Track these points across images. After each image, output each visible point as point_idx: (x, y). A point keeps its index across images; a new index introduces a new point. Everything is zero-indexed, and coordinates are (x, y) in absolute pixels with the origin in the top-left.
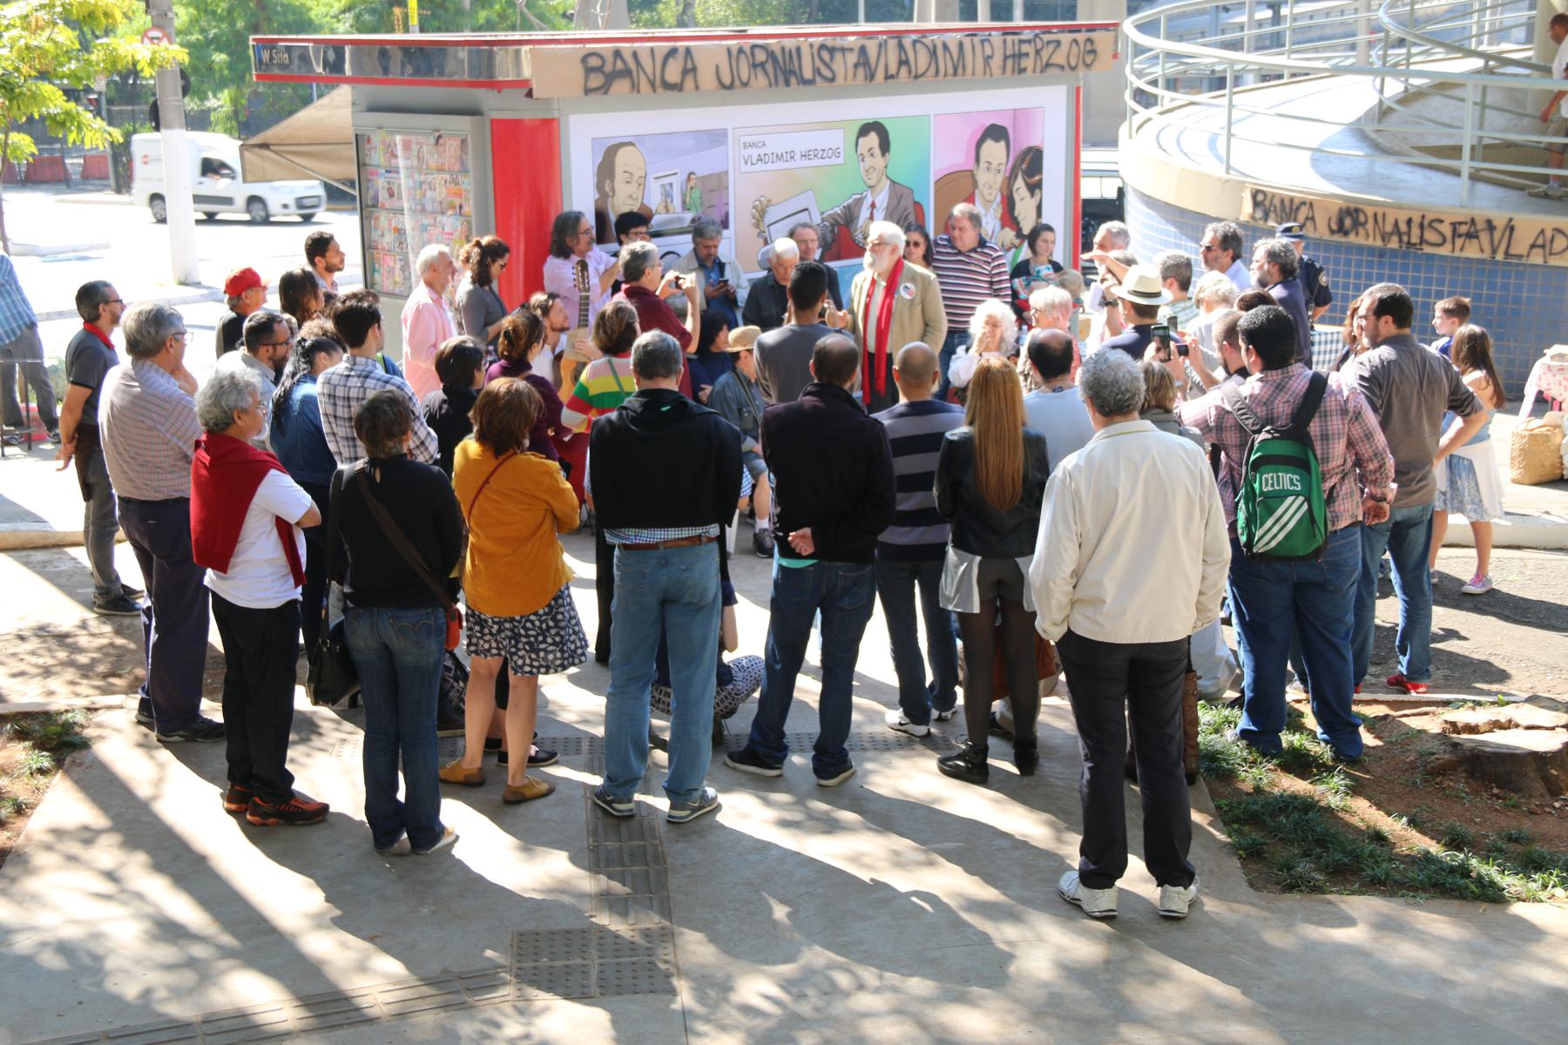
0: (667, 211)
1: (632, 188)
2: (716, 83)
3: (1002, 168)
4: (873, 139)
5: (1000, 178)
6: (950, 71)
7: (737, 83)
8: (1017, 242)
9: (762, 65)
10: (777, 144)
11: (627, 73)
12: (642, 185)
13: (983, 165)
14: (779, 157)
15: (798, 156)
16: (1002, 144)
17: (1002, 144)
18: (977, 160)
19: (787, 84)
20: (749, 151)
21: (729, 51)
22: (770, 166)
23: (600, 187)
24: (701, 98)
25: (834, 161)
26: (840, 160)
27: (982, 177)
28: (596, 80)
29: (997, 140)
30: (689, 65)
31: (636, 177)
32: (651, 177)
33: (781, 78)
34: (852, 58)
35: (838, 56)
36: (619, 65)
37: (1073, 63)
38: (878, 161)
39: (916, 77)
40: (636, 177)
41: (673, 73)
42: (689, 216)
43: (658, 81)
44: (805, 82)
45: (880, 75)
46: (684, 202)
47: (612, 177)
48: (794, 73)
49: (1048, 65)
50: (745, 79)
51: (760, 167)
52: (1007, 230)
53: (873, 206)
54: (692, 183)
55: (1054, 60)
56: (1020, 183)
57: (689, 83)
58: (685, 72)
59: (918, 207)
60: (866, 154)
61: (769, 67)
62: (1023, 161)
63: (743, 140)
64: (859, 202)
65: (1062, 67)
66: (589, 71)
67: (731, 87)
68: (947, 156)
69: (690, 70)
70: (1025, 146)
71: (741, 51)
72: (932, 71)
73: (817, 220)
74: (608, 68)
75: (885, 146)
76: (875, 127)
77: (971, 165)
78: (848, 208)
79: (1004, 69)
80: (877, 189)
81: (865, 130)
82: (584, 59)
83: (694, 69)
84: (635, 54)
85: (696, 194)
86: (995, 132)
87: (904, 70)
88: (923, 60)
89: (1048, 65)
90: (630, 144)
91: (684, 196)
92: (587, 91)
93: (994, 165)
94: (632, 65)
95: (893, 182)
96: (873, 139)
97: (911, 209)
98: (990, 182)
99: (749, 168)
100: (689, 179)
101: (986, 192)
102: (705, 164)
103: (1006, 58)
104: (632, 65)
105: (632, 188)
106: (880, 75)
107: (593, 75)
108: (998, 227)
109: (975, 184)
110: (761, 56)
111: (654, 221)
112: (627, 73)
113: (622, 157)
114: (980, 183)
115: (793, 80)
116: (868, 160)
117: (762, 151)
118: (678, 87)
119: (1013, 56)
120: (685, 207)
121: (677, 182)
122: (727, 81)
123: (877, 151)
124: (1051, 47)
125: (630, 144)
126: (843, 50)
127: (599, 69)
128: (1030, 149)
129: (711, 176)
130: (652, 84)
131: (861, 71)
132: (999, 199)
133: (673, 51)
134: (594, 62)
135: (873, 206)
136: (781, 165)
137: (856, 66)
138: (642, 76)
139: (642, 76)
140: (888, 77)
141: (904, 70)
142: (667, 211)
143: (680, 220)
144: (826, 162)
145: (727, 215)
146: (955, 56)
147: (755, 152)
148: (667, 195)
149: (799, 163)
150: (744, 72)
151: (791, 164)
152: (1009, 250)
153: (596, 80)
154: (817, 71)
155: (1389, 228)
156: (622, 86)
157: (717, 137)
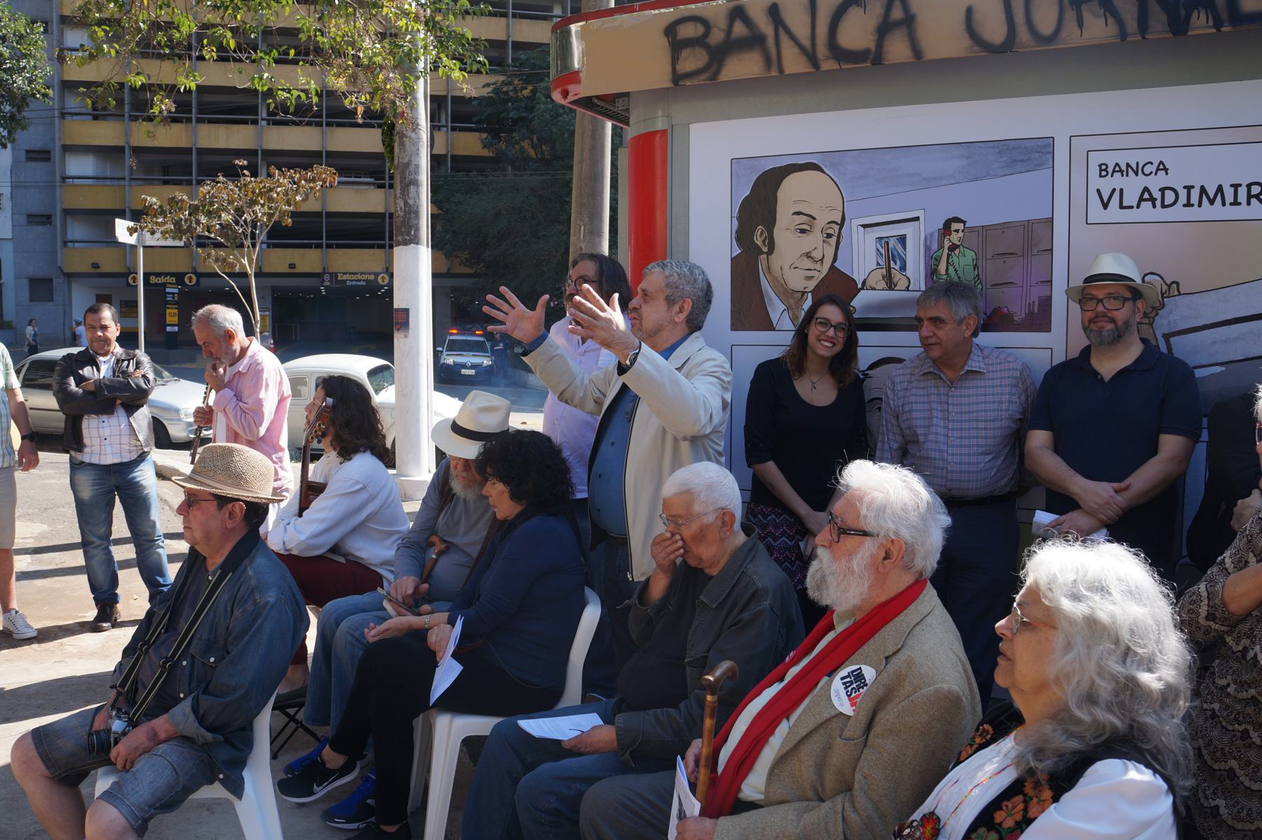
0: (891, 285)
1: (813, 241)
2: (966, 41)
7: (1023, 34)
10: (1191, 168)
11: (755, 41)
12: (836, 231)
20: (1107, 185)
22: (1178, 212)
23: (743, 236)
28: (692, 60)
30: (897, 13)
31: (821, 222)
32: (855, 223)
36: (739, 29)
40: (821, 222)
43: (822, 50)
47: (770, 222)
50: (1046, 27)
54: (955, 238)
57: (897, 49)
58: (884, 29)
63: (1096, 159)
66: (677, 47)
74: (717, 37)
83: (909, 21)
85: (964, 259)
92: (677, 78)
94: (766, 28)
102: (993, 203)
104: (766, 28)
105: (813, 241)
107: (685, 53)
112: (755, 41)
113: (791, 192)
117: (1155, 183)
122: (995, 31)
129: (1004, 227)
138: (786, 43)
139: (786, 43)
142: (891, 285)
145: (1046, 303)
147: (1132, 186)
148: (891, 256)
153: (692, 60)
156: (743, 66)
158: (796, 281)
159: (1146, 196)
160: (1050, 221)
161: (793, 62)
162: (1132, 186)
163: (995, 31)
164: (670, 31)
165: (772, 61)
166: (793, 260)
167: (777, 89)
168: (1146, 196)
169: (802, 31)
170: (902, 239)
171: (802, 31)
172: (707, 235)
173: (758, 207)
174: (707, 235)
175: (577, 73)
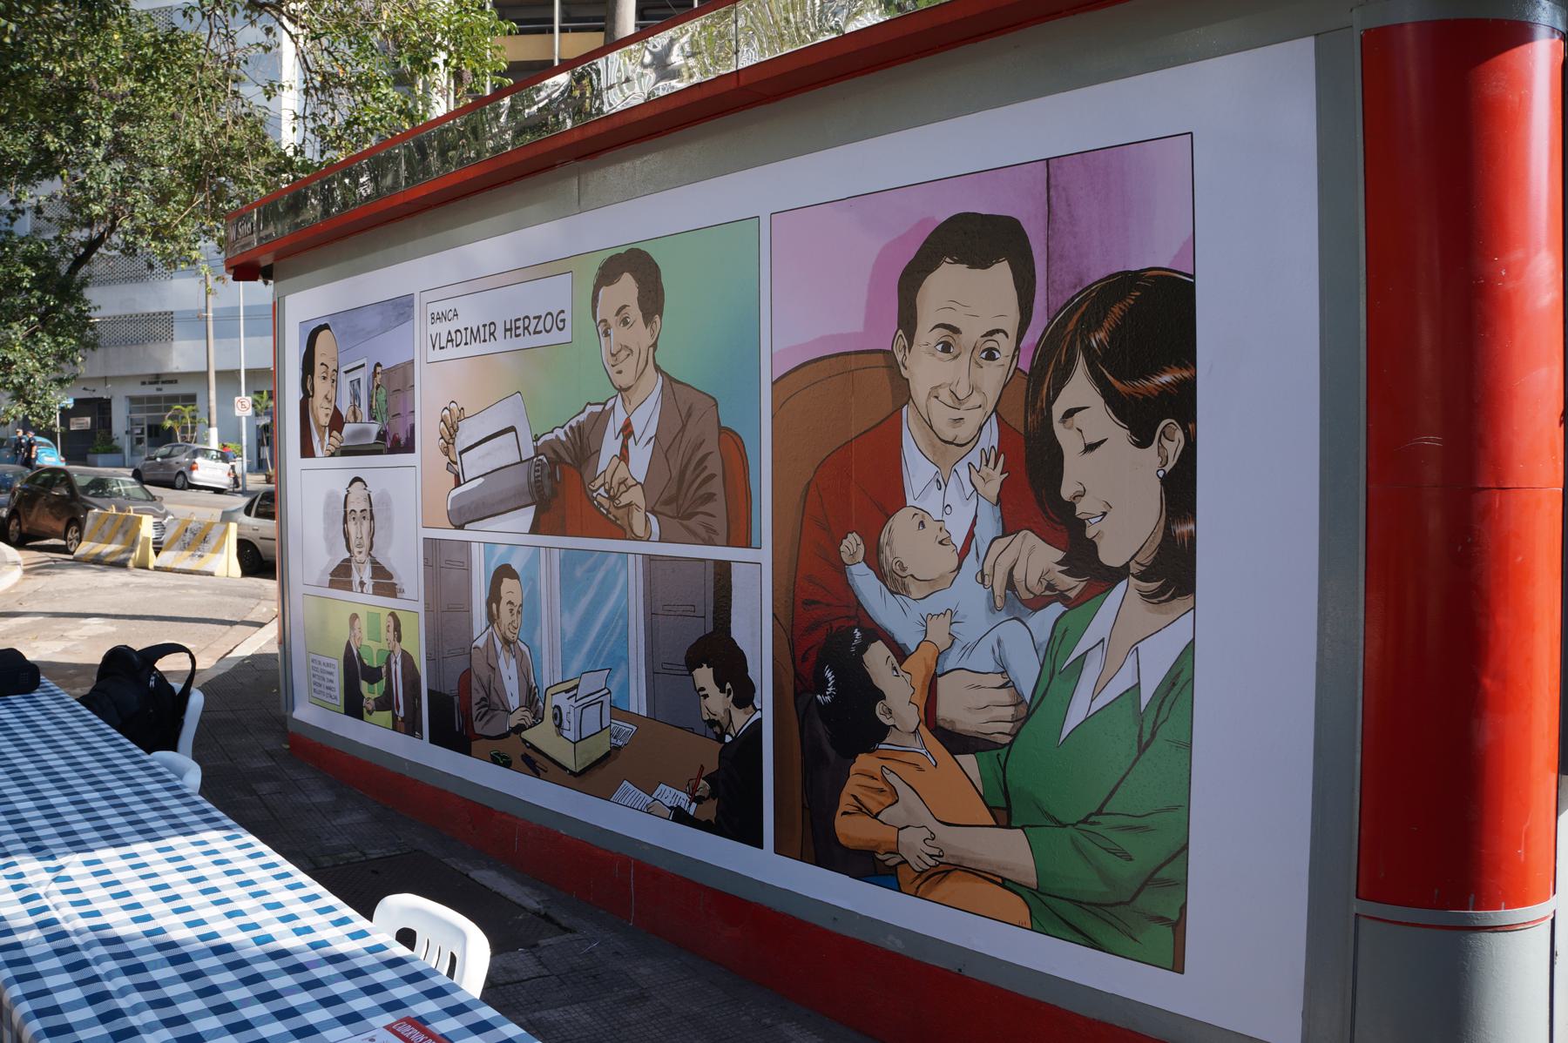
3: (1005, 346)
5: (992, 377)
8: (1073, 585)
13: (926, 334)
14: (475, 335)
15: (499, 333)
18: (908, 321)
22: (463, 351)
25: (556, 337)
26: (565, 336)
27: (925, 369)
29: (980, 261)
38: (639, 335)
42: (375, 428)
46: (370, 407)
51: (451, 352)
52: (1028, 539)
53: (627, 430)
56: (1080, 389)
59: (733, 446)
60: (612, 320)
62: (1091, 321)
64: (600, 420)
68: (812, 310)
70: (1099, 268)
73: (529, 452)
75: (652, 301)
76: (636, 265)
77: (885, 335)
78: (579, 431)
80: (636, 400)
81: (609, 271)
85: (382, 397)
86: (974, 238)
90: (326, 327)
91: (370, 397)
95: (670, 380)
96: (626, 288)
97: (711, 444)
98: (954, 385)
99: (438, 354)
100: (375, 374)
101: (941, 416)
108: (989, 526)
111: (348, 428)
114: (920, 390)
117: (453, 326)
120: (373, 418)
121: (363, 375)
123: (635, 313)
125: (326, 327)
128: (1124, 282)
132: (991, 437)
135: (627, 430)
136: (476, 348)
143: (366, 433)
144: (543, 339)
147: (443, 328)
149: (501, 343)
152: (1038, 603)
157: (401, 309)
160: (412, 362)
170: (359, 381)
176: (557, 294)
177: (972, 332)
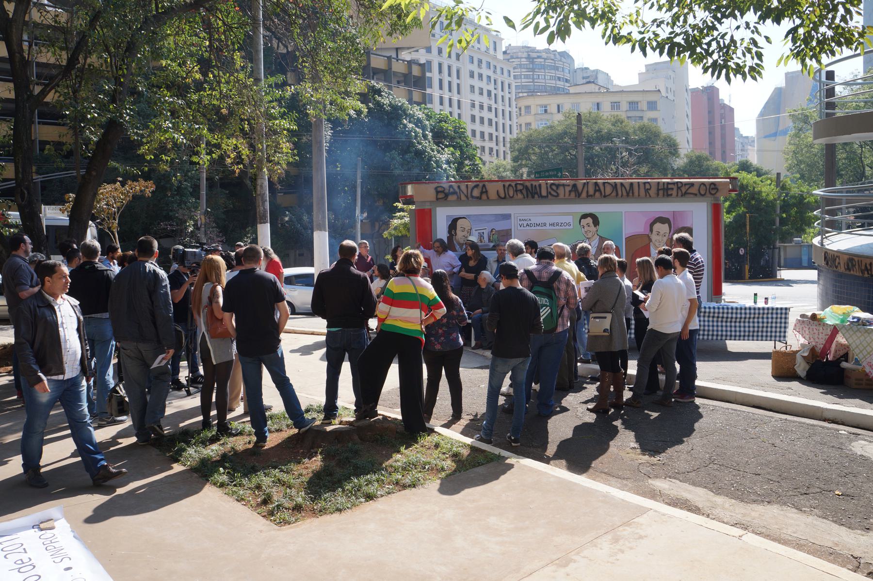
4: (589, 220)
6: (625, 193)
9: (521, 191)
10: (534, 220)
11: (455, 193)
12: (470, 232)
15: (548, 225)
16: (667, 225)
17: (667, 225)
18: (651, 230)
19: (533, 197)
21: (504, 186)
23: (450, 232)
24: (489, 202)
25: (567, 227)
27: (654, 237)
28: (441, 196)
29: (663, 223)
32: (473, 230)
33: (530, 196)
34: (568, 189)
35: (561, 188)
36: (451, 190)
37: (703, 193)
39: (605, 196)
41: (476, 193)
42: (492, 244)
44: (541, 196)
45: (584, 195)
46: (489, 239)
47: (455, 229)
48: (537, 193)
49: (686, 193)
55: (690, 191)
57: (484, 197)
58: (482, 193)
61: (524, 192)
65: (696, 195)
66: (438, 192)
67: (505, 198)
69: (484, 191)
71: (510, 185)
72: (614, 194)
77: (648, 232)
79: (658, 195)
81: (585, 216)
82: (436, 188)
83: (487, 192)
84: (459, 187)
85: (496, 237)
87: (597, 194)
88: (608, 190)
89: (686, 193)
92: (437, 199)
93: (662, 233)
94: (457, 190)
96: (589, 220)
101: (657, 244)
102: (501, 226)
103: (658, 190)
104: (457, 190)
105: (464, 234)
106: (584, 195)
109: (650, 240)
110: (520, 187)
112: (455, 193)
113: (459, 222)
114: (653, 240)
115: (536, 196)
116: (586, 228)
118: (479, 198)
119: (663, 189)
120: (490, 240)
122: (502, 195)
123: (591, 224)
124: (687, 187)
126: (564, 185)
127: (443, 192)
130: (467, 197)
131: (573, 194)
133: (476, 186)
134: (439, 189)
137: (570, 191)
140: (588, 196)
141: (597, 194)
146: (628, 188)
147: (525, 223)
148: (481, 236)
149: (548, 227)
150: (511, 193)
151: (544, 228)
154: (549, 193)
155: (863, 268)
157: (507, 217)
158: (462, 241)
159: (527, 225)
161: (463, 198)
162: (525, 223)
163: (502, 195)
164: (436, 188)
165: (459, 198)
166: (460, 235)
167: (459, 202)
168: (527, 225)
169: (465, 192)
171: (465, 192)
172: (441, 232)
173: (453, 226)
174: (441, 232)
175: (411, 196)
176: (568, 219)
177: (662, 233)
